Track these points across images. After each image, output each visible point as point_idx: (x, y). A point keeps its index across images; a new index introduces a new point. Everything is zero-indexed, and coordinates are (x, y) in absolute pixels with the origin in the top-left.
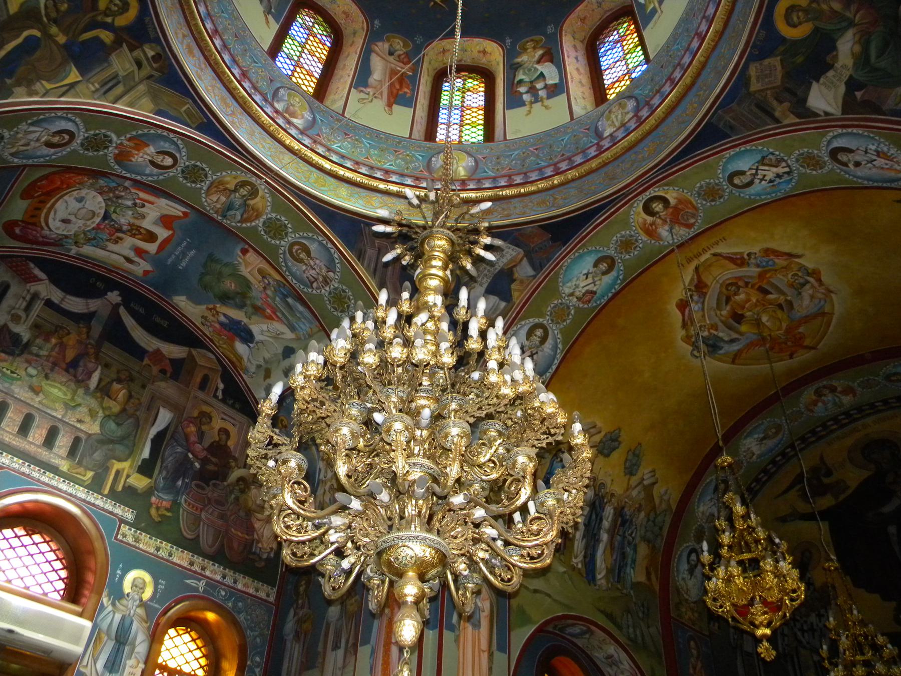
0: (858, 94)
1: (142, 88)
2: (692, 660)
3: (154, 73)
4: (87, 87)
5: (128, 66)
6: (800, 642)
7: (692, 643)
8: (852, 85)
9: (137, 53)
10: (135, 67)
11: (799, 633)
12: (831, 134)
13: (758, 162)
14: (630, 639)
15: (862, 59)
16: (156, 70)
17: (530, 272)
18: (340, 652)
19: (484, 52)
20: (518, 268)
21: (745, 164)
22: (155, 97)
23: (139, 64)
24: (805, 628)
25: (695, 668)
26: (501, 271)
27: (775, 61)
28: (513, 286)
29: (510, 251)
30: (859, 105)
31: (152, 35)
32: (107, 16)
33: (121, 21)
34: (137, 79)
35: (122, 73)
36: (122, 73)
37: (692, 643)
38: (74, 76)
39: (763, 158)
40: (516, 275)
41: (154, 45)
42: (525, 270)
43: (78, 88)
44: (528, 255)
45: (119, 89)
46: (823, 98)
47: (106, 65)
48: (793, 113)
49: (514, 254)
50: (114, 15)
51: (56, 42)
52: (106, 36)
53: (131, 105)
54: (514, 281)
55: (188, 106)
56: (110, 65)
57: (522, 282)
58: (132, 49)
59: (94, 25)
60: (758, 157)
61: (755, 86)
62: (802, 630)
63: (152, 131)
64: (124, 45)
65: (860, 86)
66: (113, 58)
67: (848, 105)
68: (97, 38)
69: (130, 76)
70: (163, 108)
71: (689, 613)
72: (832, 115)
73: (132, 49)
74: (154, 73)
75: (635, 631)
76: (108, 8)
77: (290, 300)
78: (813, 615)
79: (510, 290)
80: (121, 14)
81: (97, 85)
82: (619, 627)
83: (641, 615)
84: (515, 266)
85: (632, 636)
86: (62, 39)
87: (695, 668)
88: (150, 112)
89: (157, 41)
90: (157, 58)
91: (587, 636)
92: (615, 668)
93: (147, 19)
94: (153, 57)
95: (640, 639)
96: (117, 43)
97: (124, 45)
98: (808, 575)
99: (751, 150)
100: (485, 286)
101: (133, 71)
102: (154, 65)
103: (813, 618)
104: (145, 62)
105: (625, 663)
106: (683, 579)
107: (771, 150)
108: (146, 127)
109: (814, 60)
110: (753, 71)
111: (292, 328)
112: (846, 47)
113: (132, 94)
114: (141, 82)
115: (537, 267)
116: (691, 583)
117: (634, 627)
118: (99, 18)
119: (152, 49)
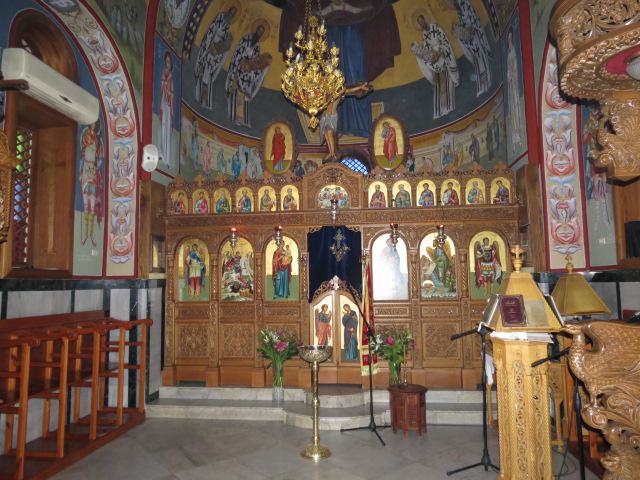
2: (166, 70)
6: (239, 86)
7: (168, 59)
11: (241, 82)
14: (117, 32)
24: (246, 79)
25: (166, 77)
37: (168, 59)
62: (243, 80)
71: (170, 36)
75: (122, 28)
78: (253, 72)
82: (108, 17)
83: (129, 16)
85: (119, 29)
87: (166, 77)
91: (74, 14)
92: (98, 55)
95: (125, 36)
98: (257, 44)
103: (252, 74)
105: (109, 51)
106: (171, 6)
116: (177, 12)
117: (121, 23)
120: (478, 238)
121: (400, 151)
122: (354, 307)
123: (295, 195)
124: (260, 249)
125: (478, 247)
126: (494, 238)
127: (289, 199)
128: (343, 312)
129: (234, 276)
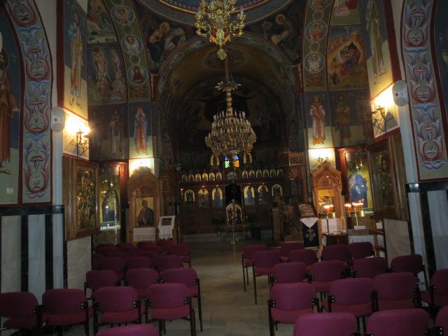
8: (282, 41)
15: (287, 38)
18: (119, 137)
21: (249, 39)
27: (271, 24)
30: (281, 45)
42: (183, 38)
44: (186, 34)
46: (275, 39)
61: (263, 26)
67: (279, 45)
77: (105, 20)
109: (279, 31)
110: (265, 22)
111: (100, 27)
112: (285, 34)
120: (274, 186)
121: (251, 162)
122: (239, 208)
123: (221, 175)
124: (210, 192)
125: (274, 189)
126: (279, 186)
127: (219, 176)
128: (236, 210)
129: (203, 200)
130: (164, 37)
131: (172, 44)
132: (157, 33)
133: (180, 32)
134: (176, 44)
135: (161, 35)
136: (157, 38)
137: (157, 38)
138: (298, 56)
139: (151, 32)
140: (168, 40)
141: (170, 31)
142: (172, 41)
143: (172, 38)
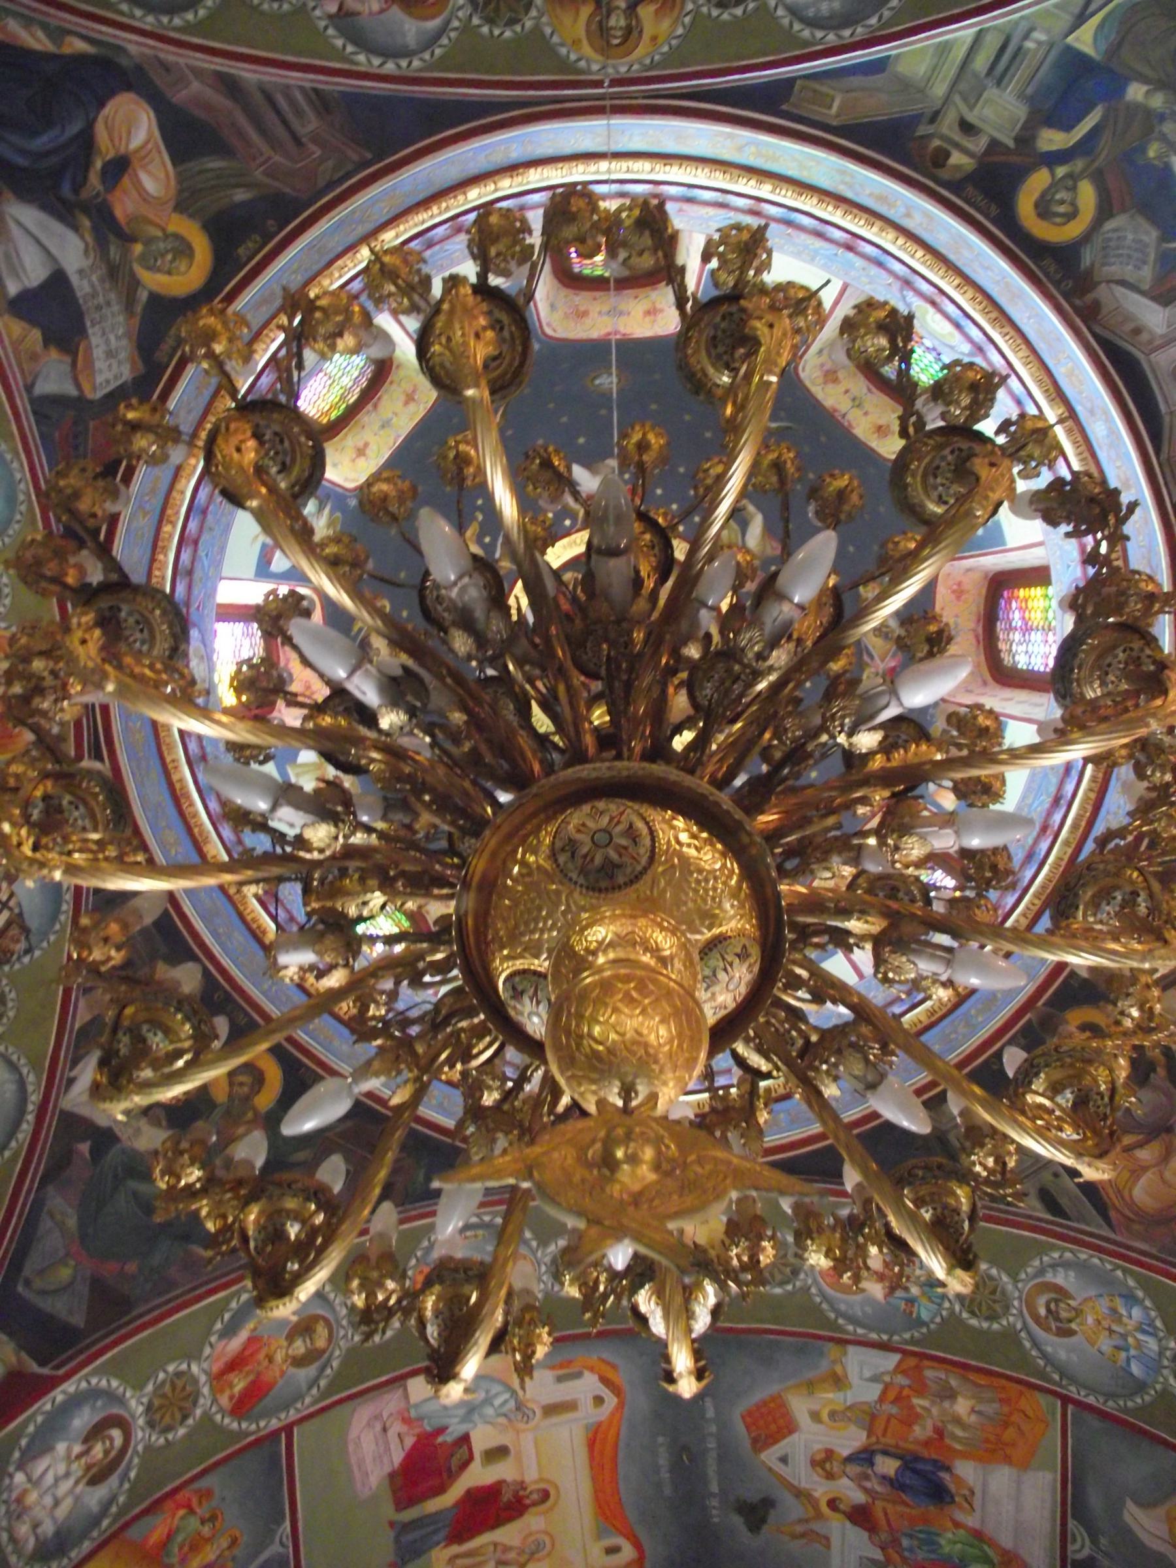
0: (84, 1148)
1: (939, 90)
3: (931, 129)
4: (1048, 31)
5: (988, 112)
9: (979, 145)
10: (971, 118)
12: (31, 1078)
13: (21, 914)
16: (929, 137)
17: (44, 387)
19: (361, 452)
20: (68, 369)
22: (905, 85)
23: (967, 128)
26: (82, 332)
28: (36, 334)
29: (109, 375)
31: (970, 190)
32: (1070, 176)
33: (1040, 180)
34: (957, 98)
35: (992, 92)
36: (992, 92)
38: (1085, 40)
39: (26, 930)
40: (54, 354)
41: (958, 176)
42: (54, 379)
43: (1066, 20)
44: (79, 403)
45: (981, 63)
47: (1030, 91)
48: (92, 1022)
49: (99, 379)
50: (1055, 185)
51: (1144, 80)
52: (1052, 140)
53: (944, 49)
54: (47, 342)
55: (833, 112)
56: (1021, 96)
57: (34, 357)
58: (994, 144)
59: (1085, 146)
60: (33, 923)
63: (873, 21)
64: (1011, 144)
65: (97, 1153)
66: (1021, 112)
68: (1067, 127)
69: (974, 97)
70: (877, 80)
72: (66, 1090)
73: (994, 144)
74: (931, 129)
76: (1074, 188)
79: (33, 322)
80: (1043, 195)
81: (1029, 45)
84: (74, 364)
86: (1136, 92)
88: (898, 56)
89: (956, 187)
90: (940, 158)
93: (994, 210)
94: (948, 155)
96: (1025, 139)
97: (1011, 144)
99: (54, 917)
100: (75, 280)
101: (971, 108)
102: (936, 143)
104: (957, 136)
107: (37, 953)
108: (889, 23)
113: (950, 70)
114: (947, 99)
115: (47, 409)
118: (1079, 164)
119: (958, 167)
130: (108, 230)
131: (35, 273)
132: (155, 179)
133: (109, 359)
134: (26, 306)
135: (124, 206)
136: (120, 166)
137: (120, 166)
138: (71, 1310)
139: (185, 135)
140: (72, 251)
141: (135, 283)
142: (58, 280)
143: (81, 287)
